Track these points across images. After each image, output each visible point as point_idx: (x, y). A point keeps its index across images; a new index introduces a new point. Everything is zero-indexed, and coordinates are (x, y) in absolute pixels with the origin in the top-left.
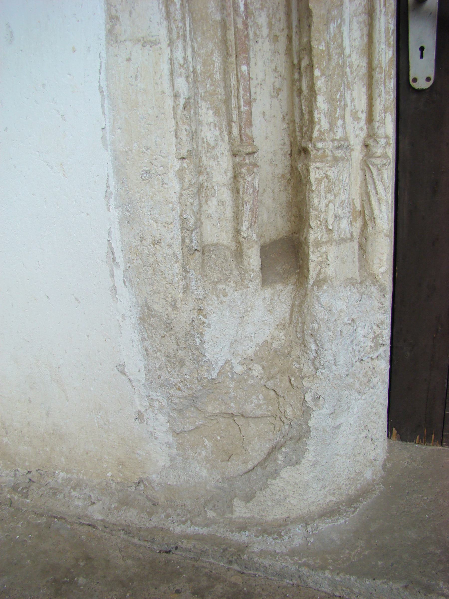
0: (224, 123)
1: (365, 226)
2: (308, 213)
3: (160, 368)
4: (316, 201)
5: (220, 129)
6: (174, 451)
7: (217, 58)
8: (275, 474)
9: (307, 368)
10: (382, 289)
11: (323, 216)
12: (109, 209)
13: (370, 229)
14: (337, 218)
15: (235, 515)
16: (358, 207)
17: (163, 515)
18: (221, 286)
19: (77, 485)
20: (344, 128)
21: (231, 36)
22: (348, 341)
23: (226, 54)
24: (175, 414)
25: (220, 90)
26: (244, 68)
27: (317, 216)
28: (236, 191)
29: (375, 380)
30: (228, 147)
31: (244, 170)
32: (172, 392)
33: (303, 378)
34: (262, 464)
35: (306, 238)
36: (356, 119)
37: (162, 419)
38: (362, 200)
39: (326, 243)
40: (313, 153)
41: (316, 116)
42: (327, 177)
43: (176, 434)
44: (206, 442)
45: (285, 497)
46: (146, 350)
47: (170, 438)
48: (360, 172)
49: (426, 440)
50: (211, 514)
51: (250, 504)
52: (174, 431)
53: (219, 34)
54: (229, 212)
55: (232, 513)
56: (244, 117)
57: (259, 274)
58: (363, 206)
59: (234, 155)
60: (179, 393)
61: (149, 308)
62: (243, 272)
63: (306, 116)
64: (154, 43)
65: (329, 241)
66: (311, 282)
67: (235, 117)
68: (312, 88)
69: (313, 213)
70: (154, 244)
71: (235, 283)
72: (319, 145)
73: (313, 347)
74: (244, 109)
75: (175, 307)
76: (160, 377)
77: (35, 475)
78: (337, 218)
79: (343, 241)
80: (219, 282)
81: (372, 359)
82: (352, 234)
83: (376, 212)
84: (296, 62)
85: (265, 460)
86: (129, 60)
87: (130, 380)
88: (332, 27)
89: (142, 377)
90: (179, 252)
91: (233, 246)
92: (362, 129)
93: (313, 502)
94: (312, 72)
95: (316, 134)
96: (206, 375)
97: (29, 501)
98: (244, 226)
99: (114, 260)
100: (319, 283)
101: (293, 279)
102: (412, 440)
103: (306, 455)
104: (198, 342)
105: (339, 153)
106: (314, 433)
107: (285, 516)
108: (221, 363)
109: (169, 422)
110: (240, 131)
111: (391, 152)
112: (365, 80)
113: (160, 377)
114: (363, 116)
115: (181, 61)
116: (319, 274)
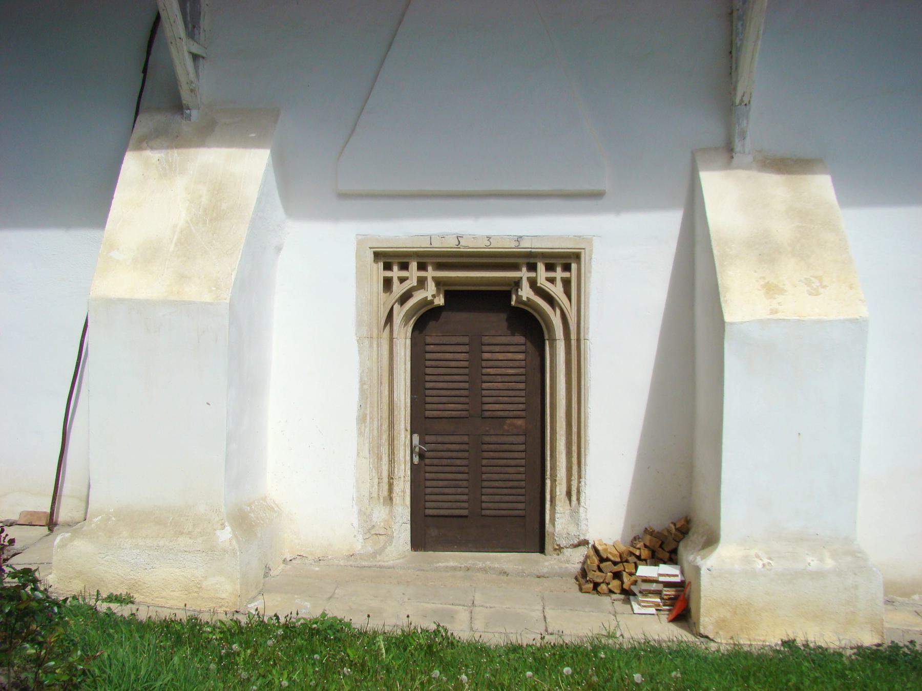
7: (376, 460)
8: (386, 548)
10: (408, 507)
21: (379, 456)
23: (378, 459)
34: (383, 546)
37: (361, 536)
47: (362, 541)
49: (421, 551)
54: (377, 490)
62: (380, 502)
64: (367, 458)
68: (394, 466)
75: (367, 509)
102: (418, 551)
111: (409, 478)
114: (404, 471)
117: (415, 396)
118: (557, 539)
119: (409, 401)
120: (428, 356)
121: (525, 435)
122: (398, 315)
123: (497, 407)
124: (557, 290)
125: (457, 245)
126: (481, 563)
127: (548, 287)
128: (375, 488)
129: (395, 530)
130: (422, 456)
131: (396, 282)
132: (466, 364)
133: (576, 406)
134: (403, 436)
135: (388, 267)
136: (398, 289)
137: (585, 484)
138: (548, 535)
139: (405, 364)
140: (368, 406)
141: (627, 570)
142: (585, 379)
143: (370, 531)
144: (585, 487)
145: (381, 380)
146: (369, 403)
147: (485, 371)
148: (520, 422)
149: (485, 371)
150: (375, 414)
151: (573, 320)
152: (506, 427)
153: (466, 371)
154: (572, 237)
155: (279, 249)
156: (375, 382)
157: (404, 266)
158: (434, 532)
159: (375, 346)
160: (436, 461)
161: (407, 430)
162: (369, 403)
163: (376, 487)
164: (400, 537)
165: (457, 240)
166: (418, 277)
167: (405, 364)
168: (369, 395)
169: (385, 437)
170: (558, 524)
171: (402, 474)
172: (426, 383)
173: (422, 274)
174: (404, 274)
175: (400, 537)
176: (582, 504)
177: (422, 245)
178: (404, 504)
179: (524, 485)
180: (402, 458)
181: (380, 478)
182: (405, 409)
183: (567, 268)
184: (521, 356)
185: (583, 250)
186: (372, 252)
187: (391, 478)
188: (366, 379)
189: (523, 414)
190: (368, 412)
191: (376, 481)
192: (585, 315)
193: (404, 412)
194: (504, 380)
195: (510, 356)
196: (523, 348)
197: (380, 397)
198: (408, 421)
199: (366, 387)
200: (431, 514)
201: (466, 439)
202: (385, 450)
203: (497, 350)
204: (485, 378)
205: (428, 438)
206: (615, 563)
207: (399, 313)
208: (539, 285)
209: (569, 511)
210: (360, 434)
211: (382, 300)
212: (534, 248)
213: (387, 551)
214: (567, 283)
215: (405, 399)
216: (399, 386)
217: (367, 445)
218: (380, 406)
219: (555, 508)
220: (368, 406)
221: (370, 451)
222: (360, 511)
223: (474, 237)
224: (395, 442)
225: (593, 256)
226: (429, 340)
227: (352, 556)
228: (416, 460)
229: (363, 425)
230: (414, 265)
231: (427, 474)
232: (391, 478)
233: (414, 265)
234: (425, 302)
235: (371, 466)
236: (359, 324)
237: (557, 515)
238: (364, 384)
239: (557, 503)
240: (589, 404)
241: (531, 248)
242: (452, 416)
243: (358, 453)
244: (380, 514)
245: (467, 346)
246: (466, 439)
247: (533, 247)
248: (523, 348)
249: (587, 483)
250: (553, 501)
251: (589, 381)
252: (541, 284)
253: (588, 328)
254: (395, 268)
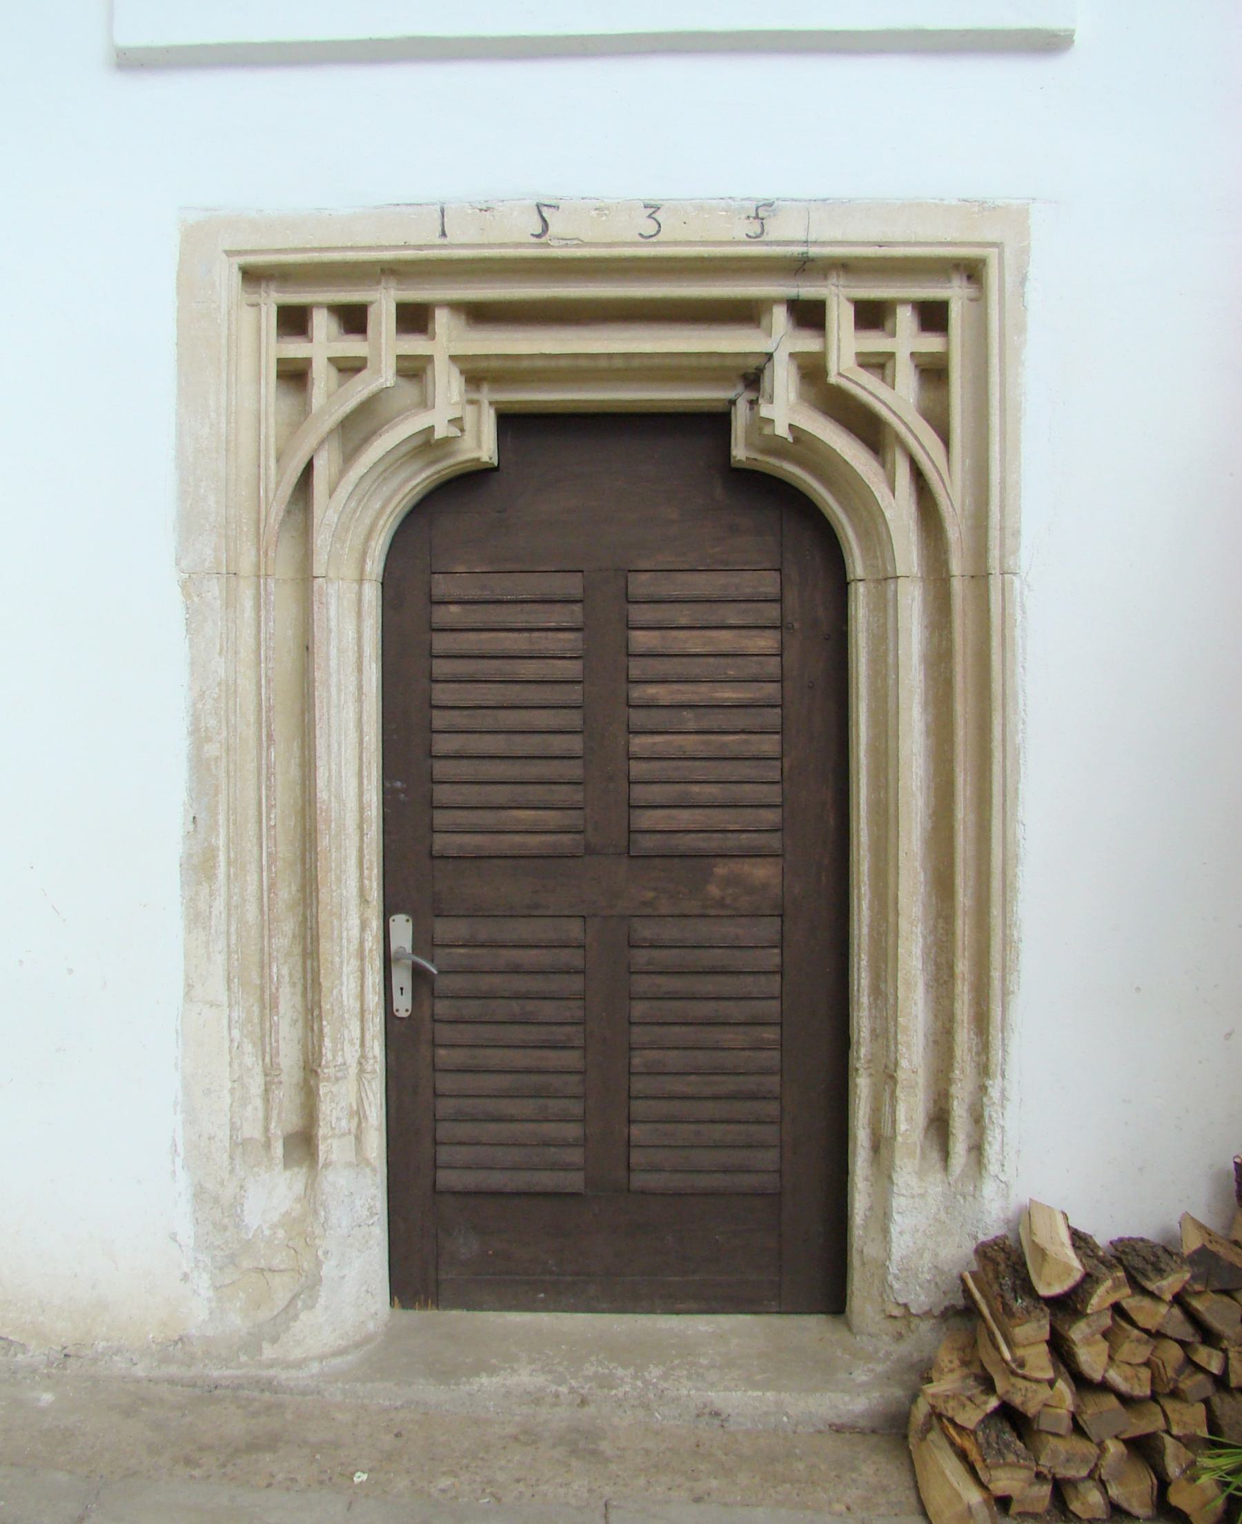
0: (260, 1053)
1: (360, 1123)
2: (318, 1115)
3: (208, 1234)
4: (324, 1108)
5: (256, 1057)
6: (214, 1304)
7: (256, 1009)
8: (295, 1318)
9: (318, 1231)
10: (374, 1170)
11: (328, 1118)
12: (175, 1114)
13: (364, 1125)
14: (338, 1119)
15: (264, 1357)
16: (355, 1108)
17: (201, 1366)
18: (256, 1169)
19: (118, 1351)
20: (343, 1056)
21: (267, 997)
22: (349, 1209)
23: (263, 1007)
24: (217, 1271)
25: (258, 1030)
26: (275, 1018)
27: (324, 1119)
28: (267, 1101)
29: (371, 1243)
30: (261, 1069)
31: (274, 1087)
32: (216, 1252)
33: (315, 1238)
35: (316, 1134)
36: (351, 1042)
37: (205, 1276)
38: (357, 1103)
39: (331, 1137)
40: (321, 1075)
41: (324, 1051)
42: (331, 1092)
43: (216, 1288)
44: (241, 1294)
45: (305, 1338)
46: (197, 1220)
47: (211, 1293)
48: (356, 1082)
49: (424, 1305)
50: (243, 1358)
51: (276, 1345)
52: (215, 1287)
53: (259, 993)
54: (261, 1115)
55: (261, 1355)
56: (274, 1051)
57: (282, 1160)
58: (358, 1107)
59: (266, 1075)
60: (222, 1253)
61: (201, 1187)
63: (317, 1048)
64: (218, 1006)
65: (333, 1136)
66: (320, 1165)
67: (268, 1049)
68: (321, 1030)
69: (321, 1116)
70: (209, 1139)
71: (266, 1167)
72: (326, 1071)
73: (322, 1213)
74: (274, 1045)
75: (222, 1184)
76: (206, 1241)
77: (71, 1350)
78: (338, 1119)
79: (343, 1135)
80: (254, 1166)
81: (369, 1226)
82: (349, 1130)
83: (368, 1112)
84: (309, 1007)
85: (287, 1306)
86: (200, 1014)
87: (180, 1246)
88: (335, 991)
89: (191, 1242)
90: (227, 1145)
91: (263, 1139)
92: (357, 1051)
93: (326, 1344)
94: (321, 1020)
95: (323, 1063)
96: (244, 1236)
97: (69, 1371)
98: (273, 1125)
99: (176, 1151)
100: (327, 1165)
101: (307, 1163)
102: (412, 1307)
103: (319, 1300)
104: (239, 1211)
105: (340, 1074)
106: (324, 1282)
107: (304, 1356)
108: (255, 1227)
109: (211, 1279)
110: (271, 1059)
112: (359, 1016)
113: (206, 1241)
114: (358, 1042)
115: (237, 1018)
116: (326, 1159)
117: (398, 784)
118: (896, 1286)
119: (373, 797)
120: (442, 642)
121: (781, 916)
122: (331, 494)
123: (685, 818)
125: (538, 236)
126: (631, 1370)
127: (866, 388)
128: (256, 1109)
129: (326, 1253)
131: (322, 376)
132: (572, 669)
133: (971, 817)
134: (354, 921)
137: (1004, 1097)
138: (864, 1264)
139: (360, 670)
140: (221, 819)
141: (1175, 1431)
142: (1004, 718)
144: (1003, 1107)
145: (269, 726)
146: (222, 808)
147: (638, 693)
148: (762, 872)
149: (638, 693)
150: (250, 844)
151: (957, 505)
152: (714, 890)
153: (574, 694)
154: (954, 202)
156: (250, 733)
158: (466, 1246)
159: (248, 604)
160: (472, 1008)
161: (367, 901)
162: (222, 808)
163: (258, 1102)
164: (344, 1277)
165: (536, 217)
166: (399, 357)
167: (360, 670)
168: (224, 781)
169: (289, 925)
170: (901, 1233)
171: (351, 1054)
172: (435, 735)
173: (415, 345)
174: (352, 347)
175: (344, 1277)
176: (993, 1168)
178: (361, 1159)
179: (777, 1089)
180: (351, 1003)
181: (271, 1073)
182: (360, 827)
184: (766, 642)
185: (996, 250)
186: (235, 269)
187: (311, 1069)
188: (212, 722)
189: (774, 841)
190: (221, 842)
191: (256, 1085)
192: (1003, 481)
193: (356, 838)
194: (705, 725)
195: (725, 640)
197: (268, 788)
198: (370, 869)
199: (212, 750)
200: (459, 1187)
201: (574, 929)
202: (285, 971)
203: (684, 621)
204: (639, 718)
205: (444, 929)
206: (1126, 1400)
208: (833, 379)
209: (939, 1189)
210: (196, 918)
211: (272, 440)
212: (815, 243)
213: (297, 1326)
215: (361, 794)
216: (335, 746)
217: (220, 959)
218: (269, 819)
219: (890, 1177)
220: (221, 819)
221: (229, 981)
222: (199, 1194)
223: (598, 204)
224: (324, 945)
225: (1032, 271)
226: (442, 586)
227: (176, 1343)
229: (205, 885)
231: (442, 1052)
232: (311, 1069)
234: (426, 445)
235: (236, 1033)
236: (189, 523)
237: (898, 1203)
238: (209, 740)
239: (898, 1162)
240: (1020, 809)
241: (806, 243)
242: (523, 852)
243: (189, 987)
245: (577, 608)
246: (574, 929)
247: (812, 238)
249: (1013, 1093)
250: (883, 1151)
251: (1021, 726)
252: (840, 374)
253: (1017, 533)
254: (322, 323)
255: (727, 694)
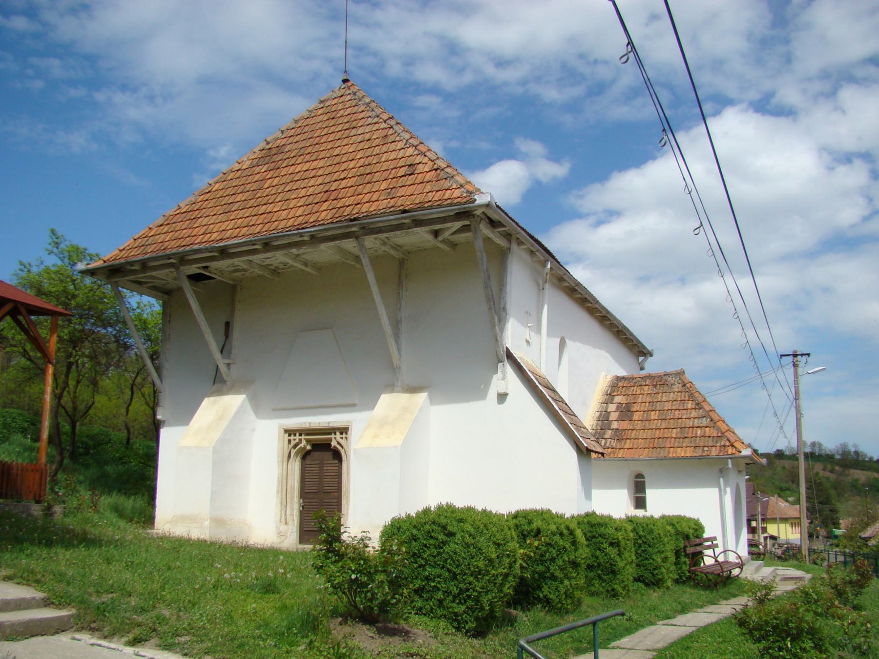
123: (329, 488)
124: (342, 442)
130: (303, 508)
135: (290, 435)
136: (293, 443)
143: (280, 534)
148: (336, 494)
155: (254, 430)
157: (295, 435)
158: (306, 537)
174: (295, 438)
177: (298, 426)
183: (346, 433)
189: (337, 491)
195: (333, 468)
196: (337, 465)
205: (306, 501)
207: (293, 452)
210: (277, 497)
214: (346, 438)
222: (276, 527)
226: (307, 463)
228: (301, 509)
230: (298, 434)
233: (298, 434)
244: (283, 528)
246: (317, 500)
248: (337, 465)
255: (333, 474)
